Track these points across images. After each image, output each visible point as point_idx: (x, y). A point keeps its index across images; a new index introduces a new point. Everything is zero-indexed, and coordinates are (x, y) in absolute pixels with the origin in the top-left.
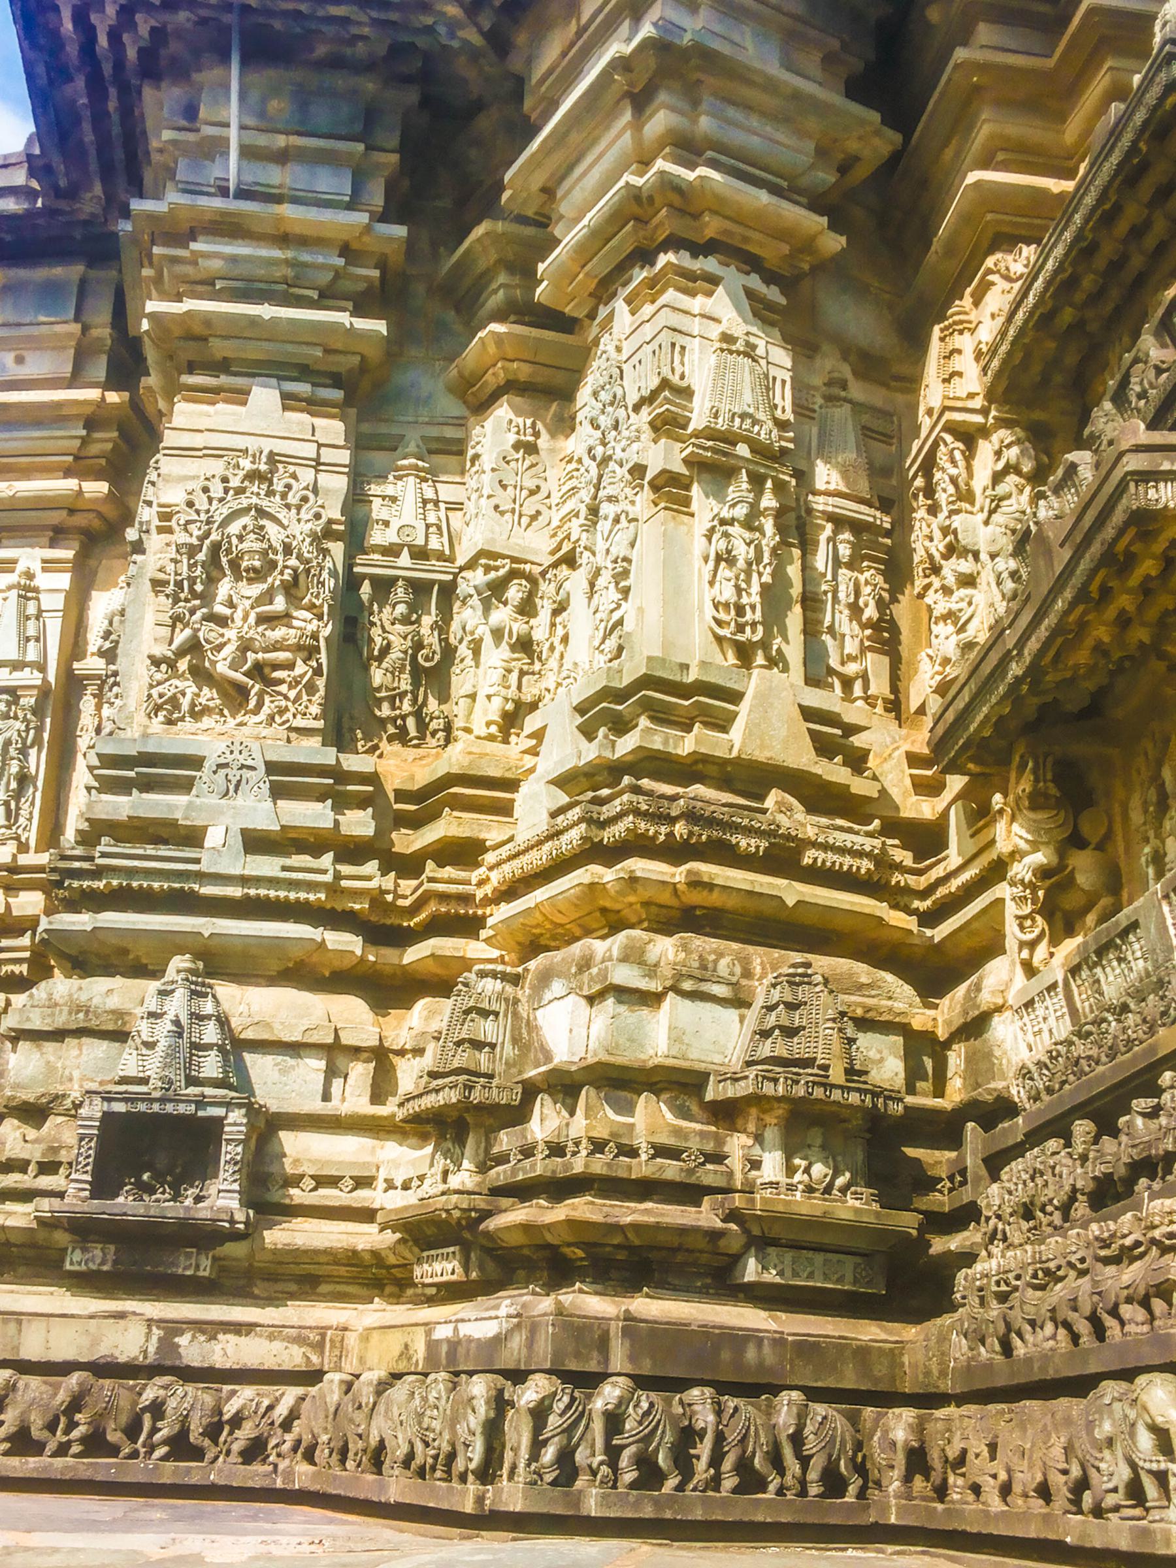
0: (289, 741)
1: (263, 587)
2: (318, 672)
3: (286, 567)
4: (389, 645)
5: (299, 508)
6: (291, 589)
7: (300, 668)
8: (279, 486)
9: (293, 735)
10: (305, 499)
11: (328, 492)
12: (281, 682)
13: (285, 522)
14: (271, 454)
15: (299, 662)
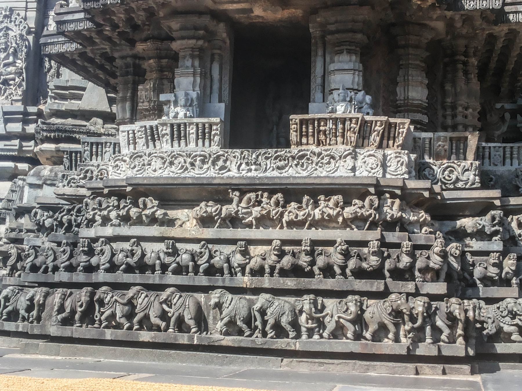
0: (12, 104)
1: (5, 54)
2: (23, 80)
3: (11, 47)
4: (51, 67)
5: (19, 25)
6: (15, 54)
7: (17, 80)
8: (13, 19)
9: (13, 102)
10: (21, 22)
11: (30, 18)
12: (11, 85)
13: (15, 31)
14: (11, 8)
15: (17, 78)
